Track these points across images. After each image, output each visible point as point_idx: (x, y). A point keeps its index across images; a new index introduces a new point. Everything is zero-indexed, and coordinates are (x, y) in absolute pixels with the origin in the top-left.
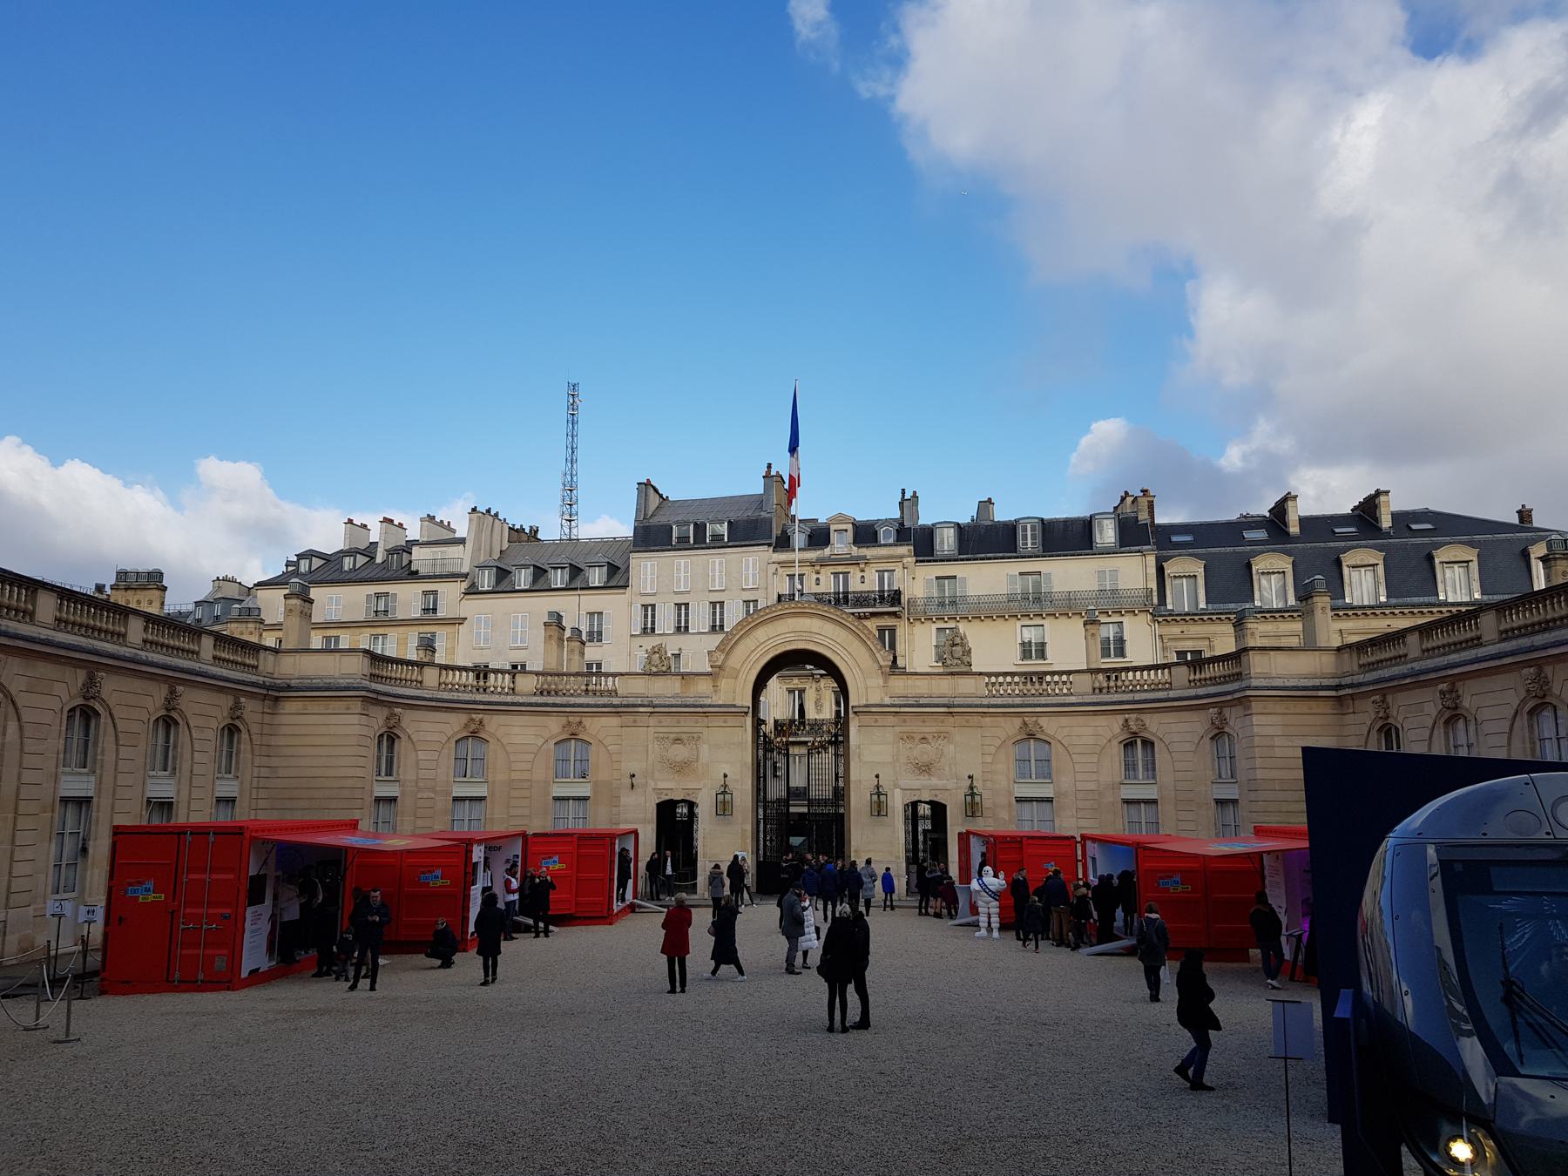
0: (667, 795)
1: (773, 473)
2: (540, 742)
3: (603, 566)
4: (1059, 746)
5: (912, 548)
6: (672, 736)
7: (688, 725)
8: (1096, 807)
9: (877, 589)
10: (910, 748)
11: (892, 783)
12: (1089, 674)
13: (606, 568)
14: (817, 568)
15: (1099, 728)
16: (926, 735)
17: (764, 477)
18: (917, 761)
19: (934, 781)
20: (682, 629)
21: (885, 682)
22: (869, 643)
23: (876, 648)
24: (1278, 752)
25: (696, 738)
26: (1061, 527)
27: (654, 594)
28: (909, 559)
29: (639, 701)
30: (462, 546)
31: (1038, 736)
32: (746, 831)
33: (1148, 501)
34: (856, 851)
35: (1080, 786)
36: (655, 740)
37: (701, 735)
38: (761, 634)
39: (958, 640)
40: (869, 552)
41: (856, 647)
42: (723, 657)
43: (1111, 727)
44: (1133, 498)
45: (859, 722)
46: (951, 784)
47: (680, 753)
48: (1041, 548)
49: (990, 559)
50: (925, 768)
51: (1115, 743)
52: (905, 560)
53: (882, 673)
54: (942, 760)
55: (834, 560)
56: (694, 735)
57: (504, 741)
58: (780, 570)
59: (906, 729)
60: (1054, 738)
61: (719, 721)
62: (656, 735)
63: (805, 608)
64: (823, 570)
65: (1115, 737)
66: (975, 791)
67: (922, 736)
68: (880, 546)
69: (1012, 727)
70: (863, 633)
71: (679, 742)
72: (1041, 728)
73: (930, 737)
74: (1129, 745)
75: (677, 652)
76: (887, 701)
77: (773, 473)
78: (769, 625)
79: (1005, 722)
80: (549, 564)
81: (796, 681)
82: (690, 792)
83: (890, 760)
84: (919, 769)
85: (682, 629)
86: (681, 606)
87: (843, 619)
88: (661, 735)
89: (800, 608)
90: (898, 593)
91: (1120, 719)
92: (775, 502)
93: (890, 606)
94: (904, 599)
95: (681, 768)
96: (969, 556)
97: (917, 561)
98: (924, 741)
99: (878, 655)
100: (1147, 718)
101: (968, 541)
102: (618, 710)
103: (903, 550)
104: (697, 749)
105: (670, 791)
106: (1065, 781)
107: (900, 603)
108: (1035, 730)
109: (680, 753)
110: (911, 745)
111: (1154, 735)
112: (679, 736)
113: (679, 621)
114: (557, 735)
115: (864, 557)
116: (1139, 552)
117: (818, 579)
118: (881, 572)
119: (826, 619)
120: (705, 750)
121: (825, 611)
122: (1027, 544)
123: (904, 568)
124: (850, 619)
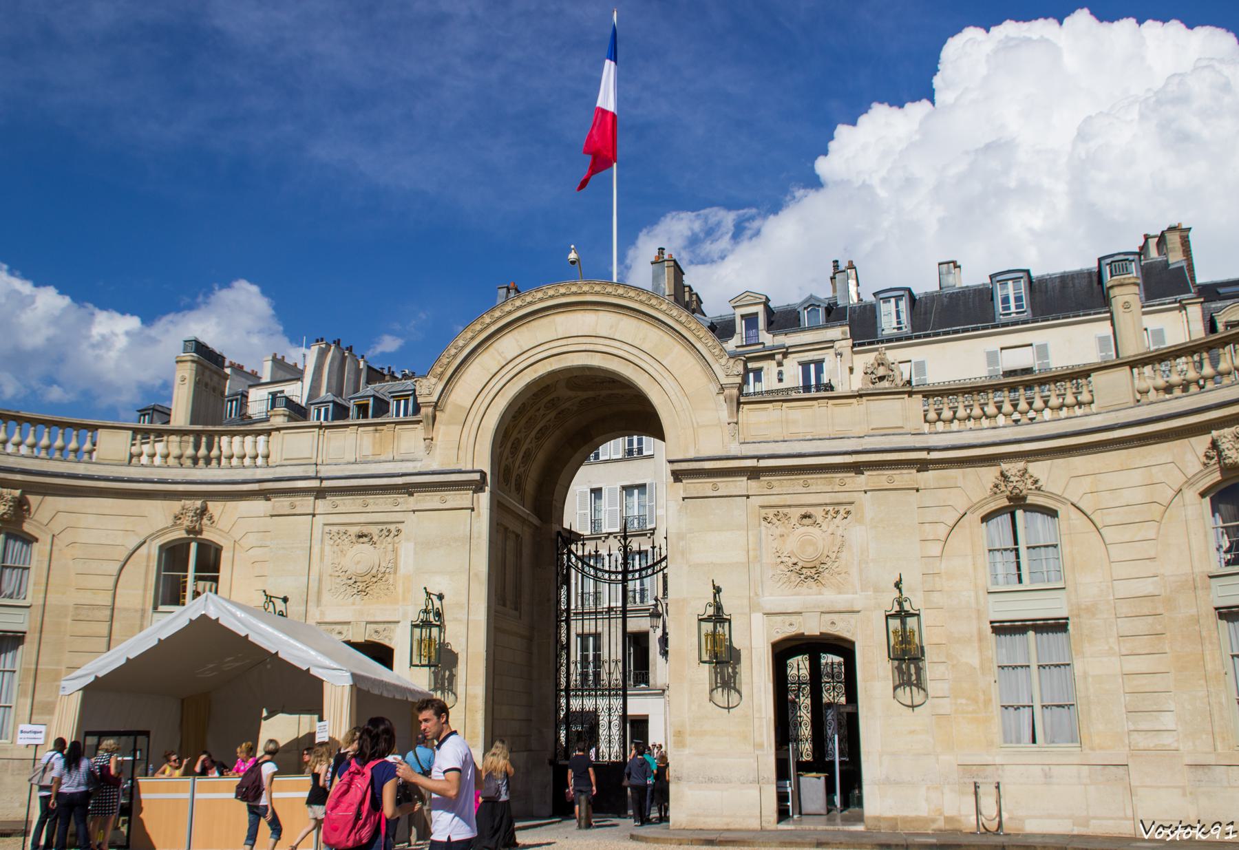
1: (666, 257)
5: (847, 329)
6: (354, 530)
7: (380, 505)
8: (1159, 629)
9: (801, 385)
10: (782, 536)
11: (746, 602)
12: (1127, 368)
15: (1154, 469)
16: (810, 510)
17: (652, 263)
19: (829, 597)
22: (699, 345)
23: (713, 354)
25: (391, 530)
26: (1057, 283)
30: (300, 383)
31: (1031, 500)
32: (475, 697)
33: (1181, 237)
35: (1123, 589)
36: (327, 537)
37: (400, 526)
41: (676, 354)
44: (1156, 239)
45: (685, 490)
47: (361, 557)
51: (1191, 495)
52: (837, 345)
54: (843, 555)
56: (389, 527)
61: (431, 500)
62: (327, 528)
63: (585, 293)
65: (1190, 482)
66: (907, 606)
67: (803, 511)
68: (804, 330)
71: (365, 539)
72: (1036, 482)
73: (818, 513)
76: (735, 449)
77: (666, 257)
78: (524, 329)
79: (964, 477)
80: (390, 393)
82: (380, 627)
83: (742, 557)
88: (335, 529)
91: (1201, 443)
92: (667, 293)
97: (854, 345)
99: (716, 367)
101: (926, 313)
103: (835, 333)
104: (395, 550)
105: (345, 627)
108: (1025, 487)
110: (781, 530)
112: (365, 530)
114: (163, 531)
118: (805, 365)
121: (620, 296)
122: (1009, 308)
124: (664, 307)
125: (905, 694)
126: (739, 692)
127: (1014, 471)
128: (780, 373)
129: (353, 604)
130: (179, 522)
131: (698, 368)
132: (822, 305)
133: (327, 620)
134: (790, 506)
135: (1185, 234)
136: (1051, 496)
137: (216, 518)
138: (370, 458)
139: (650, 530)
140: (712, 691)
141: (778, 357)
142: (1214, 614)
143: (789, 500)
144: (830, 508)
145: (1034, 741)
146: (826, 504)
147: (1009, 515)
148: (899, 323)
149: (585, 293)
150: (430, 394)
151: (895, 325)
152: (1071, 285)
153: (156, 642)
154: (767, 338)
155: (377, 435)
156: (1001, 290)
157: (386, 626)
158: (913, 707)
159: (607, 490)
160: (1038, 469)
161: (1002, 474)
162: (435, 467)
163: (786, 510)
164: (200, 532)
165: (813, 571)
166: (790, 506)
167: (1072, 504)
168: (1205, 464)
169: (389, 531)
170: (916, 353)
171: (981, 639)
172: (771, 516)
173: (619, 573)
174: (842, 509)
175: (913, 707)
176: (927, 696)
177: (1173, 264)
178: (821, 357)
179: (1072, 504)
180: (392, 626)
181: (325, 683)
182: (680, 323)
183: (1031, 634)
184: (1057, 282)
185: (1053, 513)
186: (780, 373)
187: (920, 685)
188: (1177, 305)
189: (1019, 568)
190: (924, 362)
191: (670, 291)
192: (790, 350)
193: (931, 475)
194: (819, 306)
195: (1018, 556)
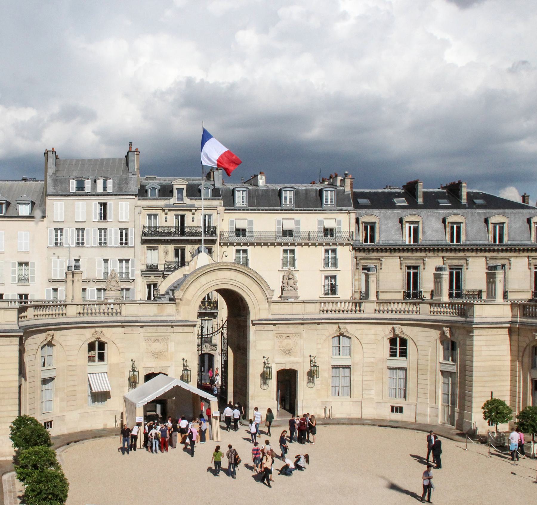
0: (150, 370)
2: (81, 343)
3: (29, 203)
4: (356, 339)
5: (222, 201)
7: (162, 331)
10: (281, 342)
13: (30, 205)
14: (166, 211)
18: (284, 349)
19: (292, 359)
20: (80, 244)
21: (269, 306)
24: (483, 353)
27: (62, 222)
28: (221, 208)
29: (134, 319)
34: (252, 396)
37: (169, 337)
38: (203, 280)
39: (291, 276)
40: (197, 203)
42: (182, 294)
43: (386, 332)
46: (300, 360)
47: (157, 347)
48: (294, 205)
49: (266, 210)
50: (288, 352)
51: (385, 339)
52: (218, 209)
53: (268, 302)
55: (176, 207)
57: (63, 344)
58: (143, 212)
59: (280, 332)
60: (352, 335)
61: (180, 329)
63: (228, 266)
64: (169, 213)
69: (333, 329)
70: (259, 280)
71: (157, 341)
72: (347, 330)
73: (291, 335)
74: (393, 341)
75: (78, 258)
81: (152, 277)
84: (285, 352)
85: (80, 244)
86: (80, 230)
87: (249, 272)
88: (147, 338)
89: (225, 266)
90: (215, 228)
92: (136, 168)
93: (210, 236)
94: (218, 233)
95: (158, 355)
96: (255, 208)
98: (288, 338)
99: (266, 292)
100: (405, 328)
102: (123, 325)
103: (217, 203)
104: (167, 345)
105: (152, 368)
106: (357, 357)
107: (216, 235)
109: (157, 347)
111: (407, 336)
112: (157, 338)
113: (78, 239)
115: (193, 206)
116: (347, 210)
117: (166, 218)
119: (252, 279)
120: (171, 346)
123: (218, 213)
125: (309, 385)
126: (268, 385)
127: (342, 327)
128: (193, 218)
129: (154, 361)
130: (94, 336)
131: (260, 292)
132: (211, 188)
133: (146, 366)
134: (283, 333)
135: (373, 225)
136: (350, 334)
137: (105, 334)
138: (157, 314)
139: (132, 280)
140: (261, 385)
141: (193, 211)
142: (387, 368)
143: (284, 332)
144: (294, 334)
145: (339, 395)
146: (293, 333)
147: (338, 337)
148: (243, 202)
149: (228, 266)
150: (179, 296)
151: (241, 203)
152: (309, 194)
153: (164, 393)
154: (187, 201)
155: (159, 307)
156: (284, 194)
157: (165, 368)
158: (311, 388)
159: (112, 261)
160: (348, 326)
161: (339, 327)
162: (180, 319)
163: (282, 335)
164: (100, 338)
165: (289, 352)
166: (283, 333)
167: (356, 337)
168: (390, 332)
169: (165, 339)
170: (250, 216)
171: (329, 369)
172: (278, 337)
173: (200, 335)
174: (297, 335)
175: (311, 388)
176: (315, 385)
177: (346, 192)
178: (211, 213)
179: (356, 337)
180: (167, 368)
181: (211, 401)
182: (257, 278)
183: (341, 369)
184: (304, 192)
185: (350, 338)
186: (193, 218)
187: (313, 382)
188: (347, 212)
189: (339, 351)
190: (252, 220)
191: (137, 167)
192: (198, 209)
193: (320, 325)
194: (209, 188)
195: (339, 348)
